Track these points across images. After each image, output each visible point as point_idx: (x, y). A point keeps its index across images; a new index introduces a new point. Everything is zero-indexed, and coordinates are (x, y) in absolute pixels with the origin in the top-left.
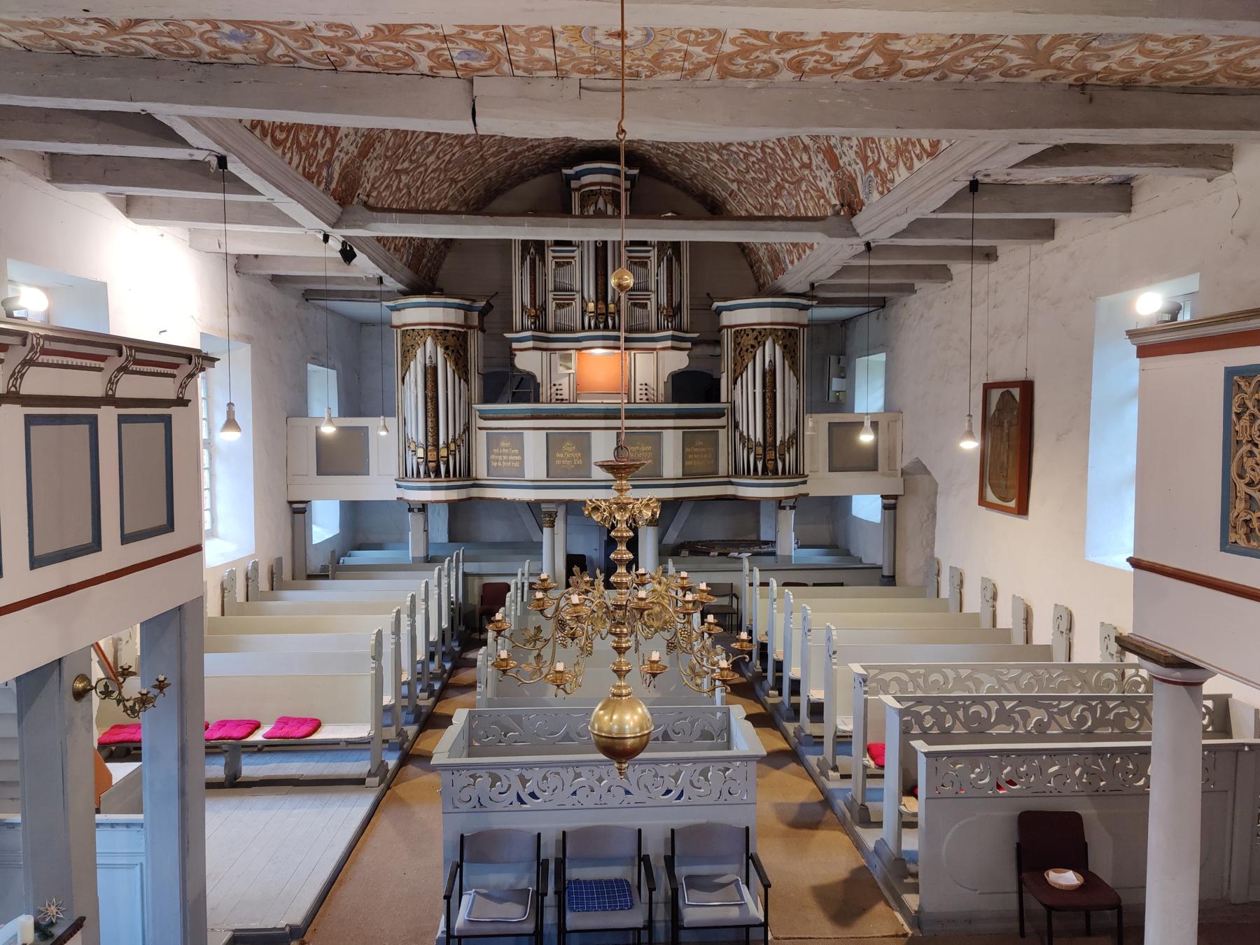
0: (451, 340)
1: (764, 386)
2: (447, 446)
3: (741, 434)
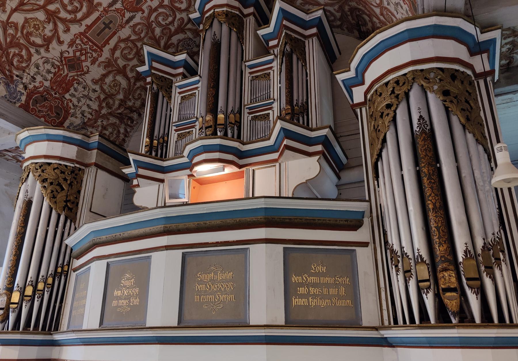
0: (50, 174)
1: (416, 162)
2: (22, 292)
3: (392, 251)
